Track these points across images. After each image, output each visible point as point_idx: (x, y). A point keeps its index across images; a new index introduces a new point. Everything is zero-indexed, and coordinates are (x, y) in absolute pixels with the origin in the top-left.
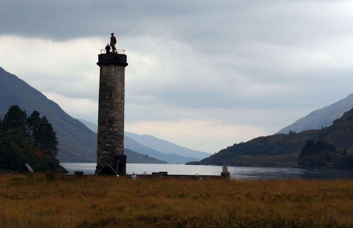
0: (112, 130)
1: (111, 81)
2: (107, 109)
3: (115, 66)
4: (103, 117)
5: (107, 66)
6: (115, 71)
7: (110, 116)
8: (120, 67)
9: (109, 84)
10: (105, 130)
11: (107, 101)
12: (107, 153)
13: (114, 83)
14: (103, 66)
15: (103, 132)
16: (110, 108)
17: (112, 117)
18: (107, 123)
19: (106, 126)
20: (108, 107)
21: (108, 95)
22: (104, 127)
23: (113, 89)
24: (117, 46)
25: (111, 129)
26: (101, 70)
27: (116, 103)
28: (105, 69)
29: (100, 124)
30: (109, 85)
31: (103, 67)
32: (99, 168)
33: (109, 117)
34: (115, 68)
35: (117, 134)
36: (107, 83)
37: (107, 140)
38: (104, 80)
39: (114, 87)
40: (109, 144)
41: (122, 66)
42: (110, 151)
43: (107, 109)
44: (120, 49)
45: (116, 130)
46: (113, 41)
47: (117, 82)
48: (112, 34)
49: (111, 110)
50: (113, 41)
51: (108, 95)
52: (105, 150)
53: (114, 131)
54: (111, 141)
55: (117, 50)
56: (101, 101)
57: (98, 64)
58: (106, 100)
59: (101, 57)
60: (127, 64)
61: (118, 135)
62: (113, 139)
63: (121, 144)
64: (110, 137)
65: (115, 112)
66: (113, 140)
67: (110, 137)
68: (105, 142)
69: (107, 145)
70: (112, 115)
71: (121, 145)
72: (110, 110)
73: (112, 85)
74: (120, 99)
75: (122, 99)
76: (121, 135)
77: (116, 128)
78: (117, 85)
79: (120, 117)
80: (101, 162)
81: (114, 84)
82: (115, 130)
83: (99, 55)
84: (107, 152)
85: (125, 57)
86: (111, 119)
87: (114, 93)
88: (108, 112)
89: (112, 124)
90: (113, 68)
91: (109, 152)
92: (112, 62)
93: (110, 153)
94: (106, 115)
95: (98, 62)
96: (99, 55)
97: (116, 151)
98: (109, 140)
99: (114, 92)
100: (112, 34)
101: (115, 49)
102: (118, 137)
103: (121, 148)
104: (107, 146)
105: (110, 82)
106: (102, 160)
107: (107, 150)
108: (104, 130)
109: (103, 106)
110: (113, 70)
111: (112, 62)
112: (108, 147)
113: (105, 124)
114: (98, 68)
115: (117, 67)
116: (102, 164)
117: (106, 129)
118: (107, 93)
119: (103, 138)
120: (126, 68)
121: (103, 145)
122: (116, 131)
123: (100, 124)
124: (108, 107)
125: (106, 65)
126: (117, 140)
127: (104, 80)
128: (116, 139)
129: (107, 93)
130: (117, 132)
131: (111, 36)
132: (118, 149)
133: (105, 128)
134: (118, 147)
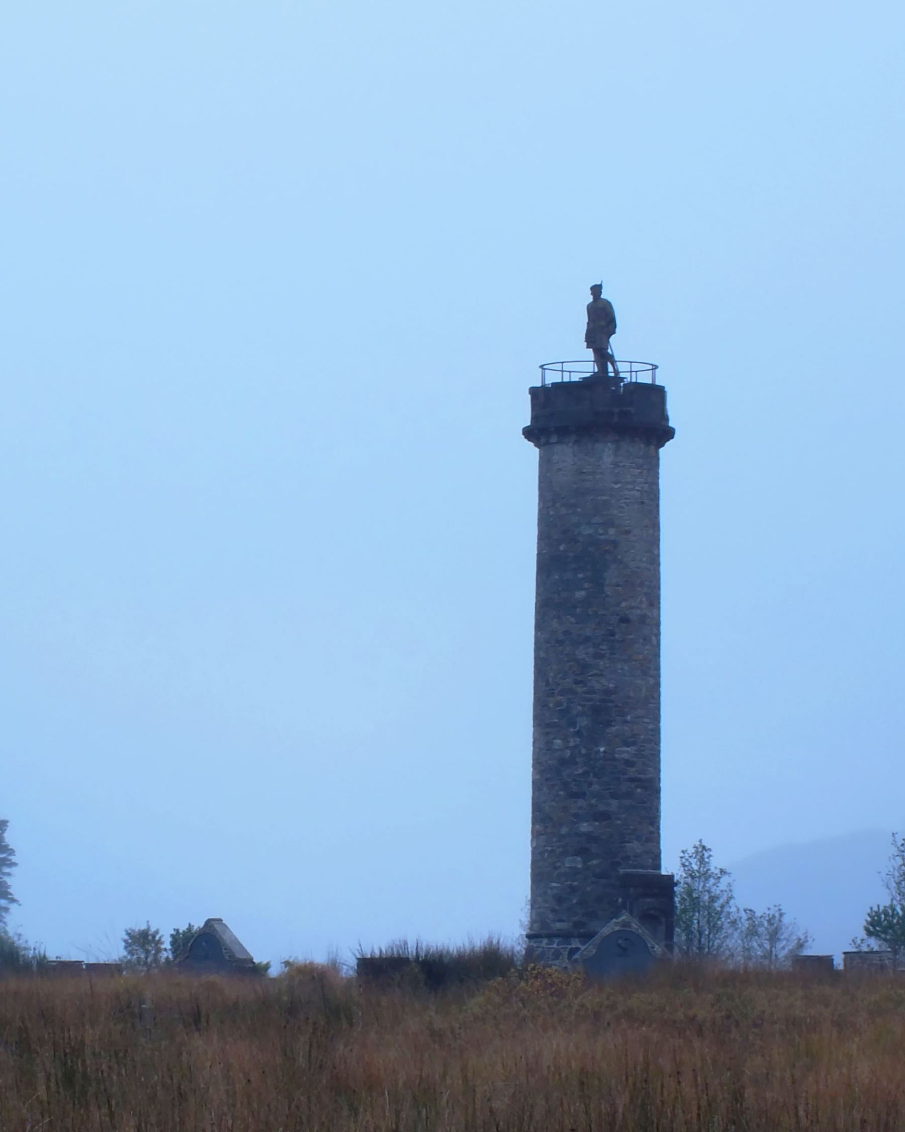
0: (604, 752)
2: (582, 653)
4: (562, 693)
5: (576, 442)
6: (616, 465)
7: (598, 686)
9: (586, 531)
11: (578, 610)
14: (557, 443)
15: (564, 762)
17: (608, 692)
18: (583, 722)
19: (578, 734)
20: (587, 639)
21: (586, 585)
22: (565, 739)
24: (617, 345)
25: (602, 749)
26: (545, 464)
28: (566, 453)
29: (548, 725)
30: (590, 536)
31: (558, 448)
33: (592, 691)
35: (632, 772)
37: (581, 802)
38: (563, 511)
39: (615, 543)
40: (596, 820)
41: (648, 443)
43: (582, 653)
44: (631, 356)
45: (625, 752)
46: (601, 322)
48: (596, 290)
49: (602, 656)
50: (601, 322)
51: (586, 585)
52: (578, 853)
53: (615, 759)
54: (602, 808)
55: (621, 367)
57: (529, 433)
59: (545, 399)
60: (669, 434)
61: (632, 780)
62: (614, 796)
64: (596, 787)
65: (619, 666)
67: (596, 787)
68: (576, 815)
69: (585, 827)
70: (604, 681)
72: (599, 656)
73: (606, 533)
74: (641, 602)
77: (626, 744)
78: (628, 532)
79: (644, 691)
80: (553, 911)
81: (612, 531)
82: (623, 752)
83: (534, 392)
85: (654, 395)
86: (603, 701)
88: (584, 667)
89: (609, 724)
90: (606, 454)
91: (595, 862)
94: (577, 682)
95: (528, 423)
96: (534, 392)
97: (627, 858)
98: (594, 801)
100: (596, 290)
101: (611, 359)
102: (637, 787)
103: (648, 840)
105: (594, 520)
106: (559, 900)
107: (582, 852)
108: (568, 753)
109: (561, 637)
112: (590, 838)
113: (573, 724)
114: (531, 453)
116: (560, 921)
117: (576, 747)
119: (562, 793)
120: (667, 453)
122: (625, 756)
125: (574, 437)
126: (627, 802)
129: (581, 576)
130: (629, 763)
131: (590, 299)
132: (634, 846)
134: (638, 839)
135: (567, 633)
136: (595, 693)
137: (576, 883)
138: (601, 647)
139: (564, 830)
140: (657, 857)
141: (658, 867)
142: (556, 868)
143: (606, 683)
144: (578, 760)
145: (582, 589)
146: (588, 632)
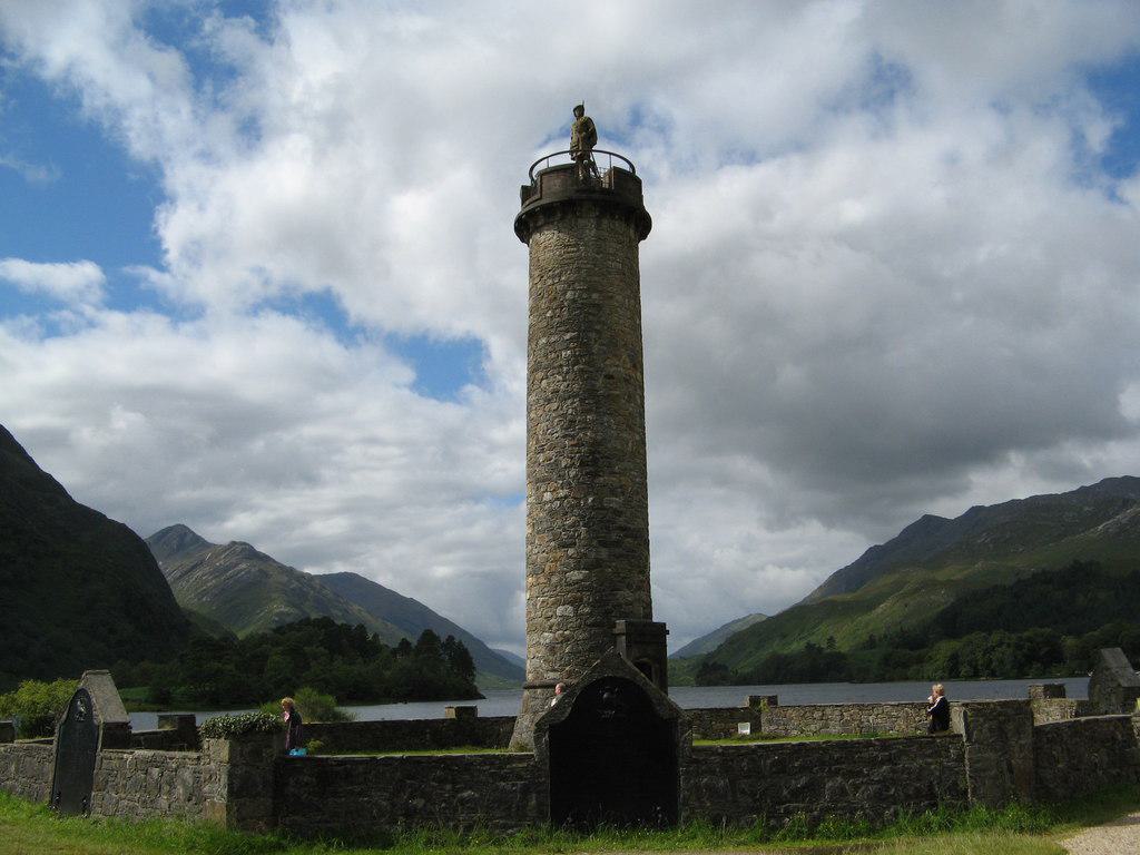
3: (599, 218)
8: (619, 226)
12: (576, 614)
13: (596, 291)
27: (610, 377)
29: (538, 481)
32: (539, 691)
34: (598, 227)
35: (621, 521)
45: (615, 502)
47: (612, 285)
48: (580, 110)
50: (586, 134)
53: (604, 509)
56: (540, 375)
61: (623, 529)
62: (603, 544)
63: (640, 572)
65: (605, 419)
66: (604, 553)
75: (634, 366)
77: (613, 493)
79: (630, 444)
81: (595, 296)
87: (598, 332)
94: (565, 436)
97: (620, 605)
99: (598, 327)
100: (580, 110)
102: (626, 536)
103: (639, 588)
106: (552, 649)
115: (605, 222)
116: (554, 670)
119: (553, 544)
123: (538, 481)
127: (550, 282)
128: (617, 544)
130: (618, 513)
132: (625, 595)
134: (629, 586)
139: (555, 579)
140: (648, 605)
141: (649, 615)
142: (548, 618)
145: (567, 348)
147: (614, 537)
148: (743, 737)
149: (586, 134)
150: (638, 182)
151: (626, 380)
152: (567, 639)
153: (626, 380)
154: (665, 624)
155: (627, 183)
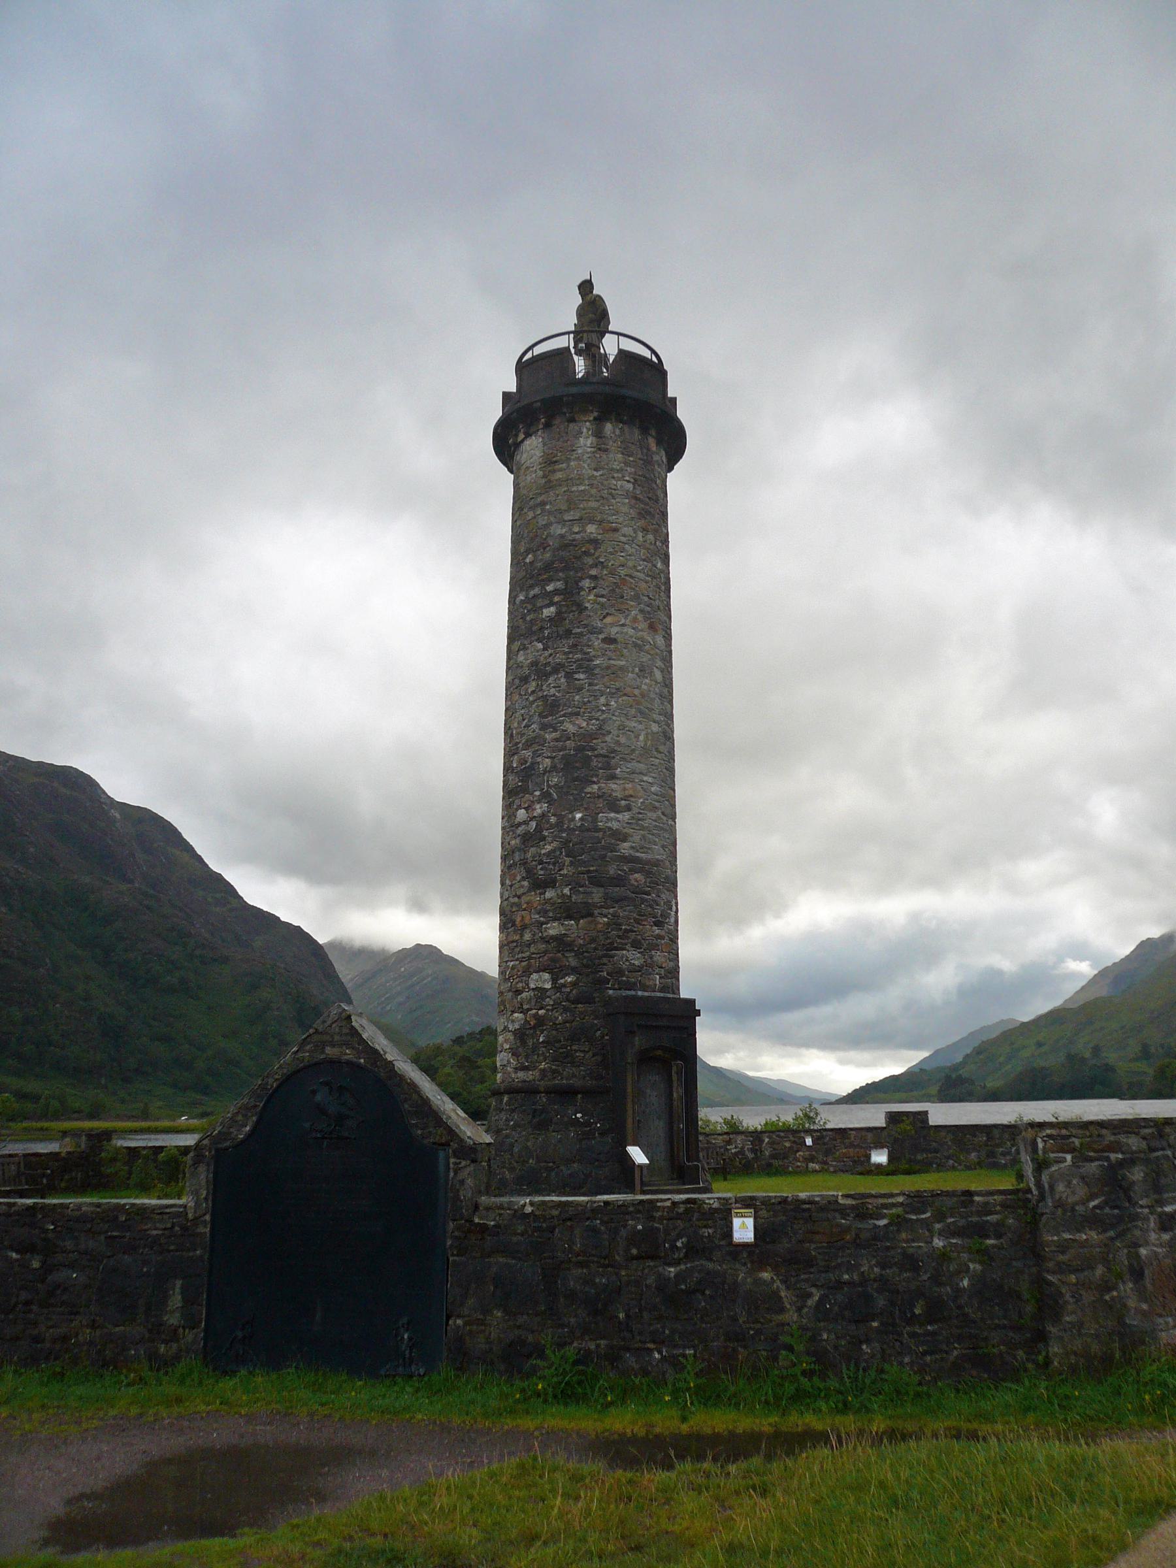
0: (581, 819)
1: (571, 505)
3: (600, 420)
4: (527, 746)
5: (548, 425)
7: (571, 728)
9: (558, 530)
10: (539, 829)
12: (557, 988)
13: (591, 521)
16: (569, 676)
19: (546, 796)
21: (556, 599)
23: (586, 553)
25: (578, 816)
27: (610, 640)
30: (562, 536)
34: (598, 434)
35: (625, 848)
36: (547, 526)
37: (550, 894)
38: (531, 514)
39: (595, 542)
40: (570, 917)
42: (574, 970)
47: (617, 513)
48: (586, 287)
53: (598, 830)
56: (517, 644)
58: (542, 629)
62: (596, 882)
63: (658, 924)
66: (597, 895)
71: (656, 930)
74: (635, 620)
75: (652, 627)
76: (657, 863)
77: (613, 806)
78: (616, 530)
79: (641, 738)
81: (591, 529)
82: (609, 820)
84: (554, 980)
87: (594, 578)
91: (569, 979)
92: (593, 425)
93: (574, 984)
94: (544, 727)
97: (620, 972)
98: (566, 891)
99: (593, 572)
100: (586, 287)
102: (633, 871)
104: (552, 937)
108: (533, 824)
110: (586, 442)
111: (593, 425)
112: (561, 942)
115: (608, 427)
117: (543, 815)
118: (549, 588)
119: (526, 883)
121: (527, 937)
122: (615, 825)
124: (556, 670)
127: (531, 514)
128: (619, 881)
129: (549, 588)
133: (539, 809)
134: (636, 945)
135: (534, 664)
136: (569, 739)
137: (541, 1012)
138: (576, 676)
140: (674, 972)
141: (676, 989)
142: (518, 992)
143: (584, 724)
144: (546, 833)
145: (551, 604)
146: (560, 659)
147: (612, 870)
148: (879, 1169)
149: (593, 315)
150: (664, 374)
151: (635, 645)
152: (540, 1022)
153: (635, 645)
154: (694, 1001)
155: (646, 372)
